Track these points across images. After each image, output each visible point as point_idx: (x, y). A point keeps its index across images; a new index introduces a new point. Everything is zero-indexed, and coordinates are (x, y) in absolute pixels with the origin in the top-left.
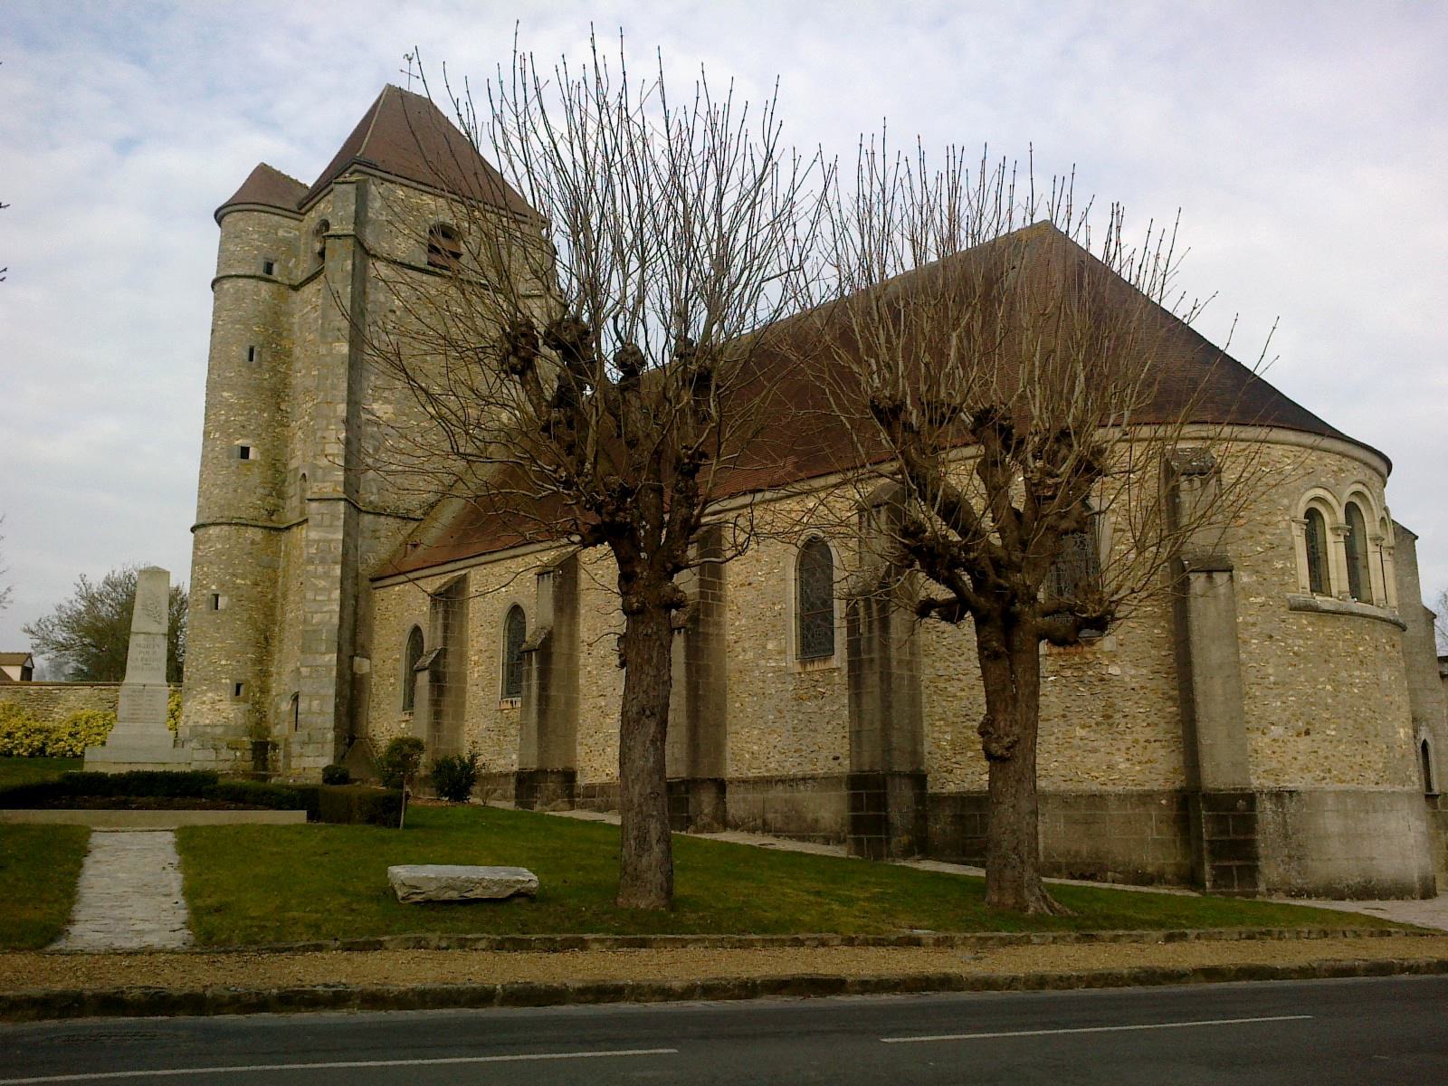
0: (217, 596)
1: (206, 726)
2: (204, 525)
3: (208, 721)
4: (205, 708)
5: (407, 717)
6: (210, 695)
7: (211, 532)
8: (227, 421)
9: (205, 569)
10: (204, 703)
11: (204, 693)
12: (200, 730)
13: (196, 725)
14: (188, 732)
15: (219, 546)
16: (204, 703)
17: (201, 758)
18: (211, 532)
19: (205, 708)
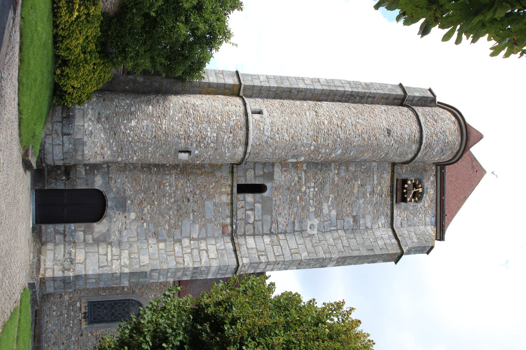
0: (189, 152)
1: (83, 151)
2: (247, 144)
3: (86, 152)
4: (98, 150)
5: (83, 310)
6: (109, 152)
7: (240, 148)
8: (320, 153)
9: (212, 145)
10: (102, 148)
11: (111, 148)
12: (80, 148)
13: (84, 144)
14: (78, 137)
15: (228, 155)
16: (102, 148)
17: (55, 152)
18: (240, 148)
19: (98, 150)
